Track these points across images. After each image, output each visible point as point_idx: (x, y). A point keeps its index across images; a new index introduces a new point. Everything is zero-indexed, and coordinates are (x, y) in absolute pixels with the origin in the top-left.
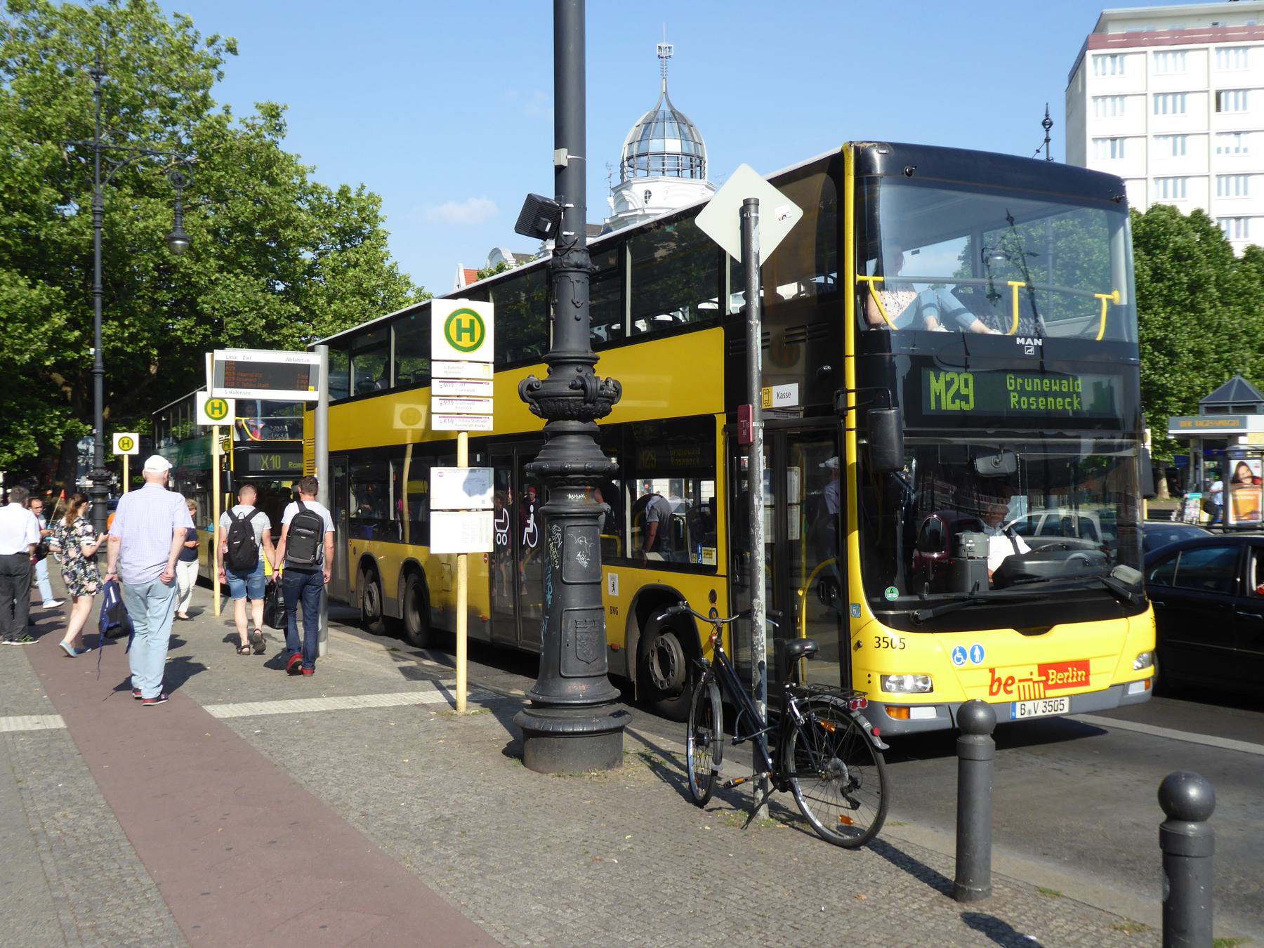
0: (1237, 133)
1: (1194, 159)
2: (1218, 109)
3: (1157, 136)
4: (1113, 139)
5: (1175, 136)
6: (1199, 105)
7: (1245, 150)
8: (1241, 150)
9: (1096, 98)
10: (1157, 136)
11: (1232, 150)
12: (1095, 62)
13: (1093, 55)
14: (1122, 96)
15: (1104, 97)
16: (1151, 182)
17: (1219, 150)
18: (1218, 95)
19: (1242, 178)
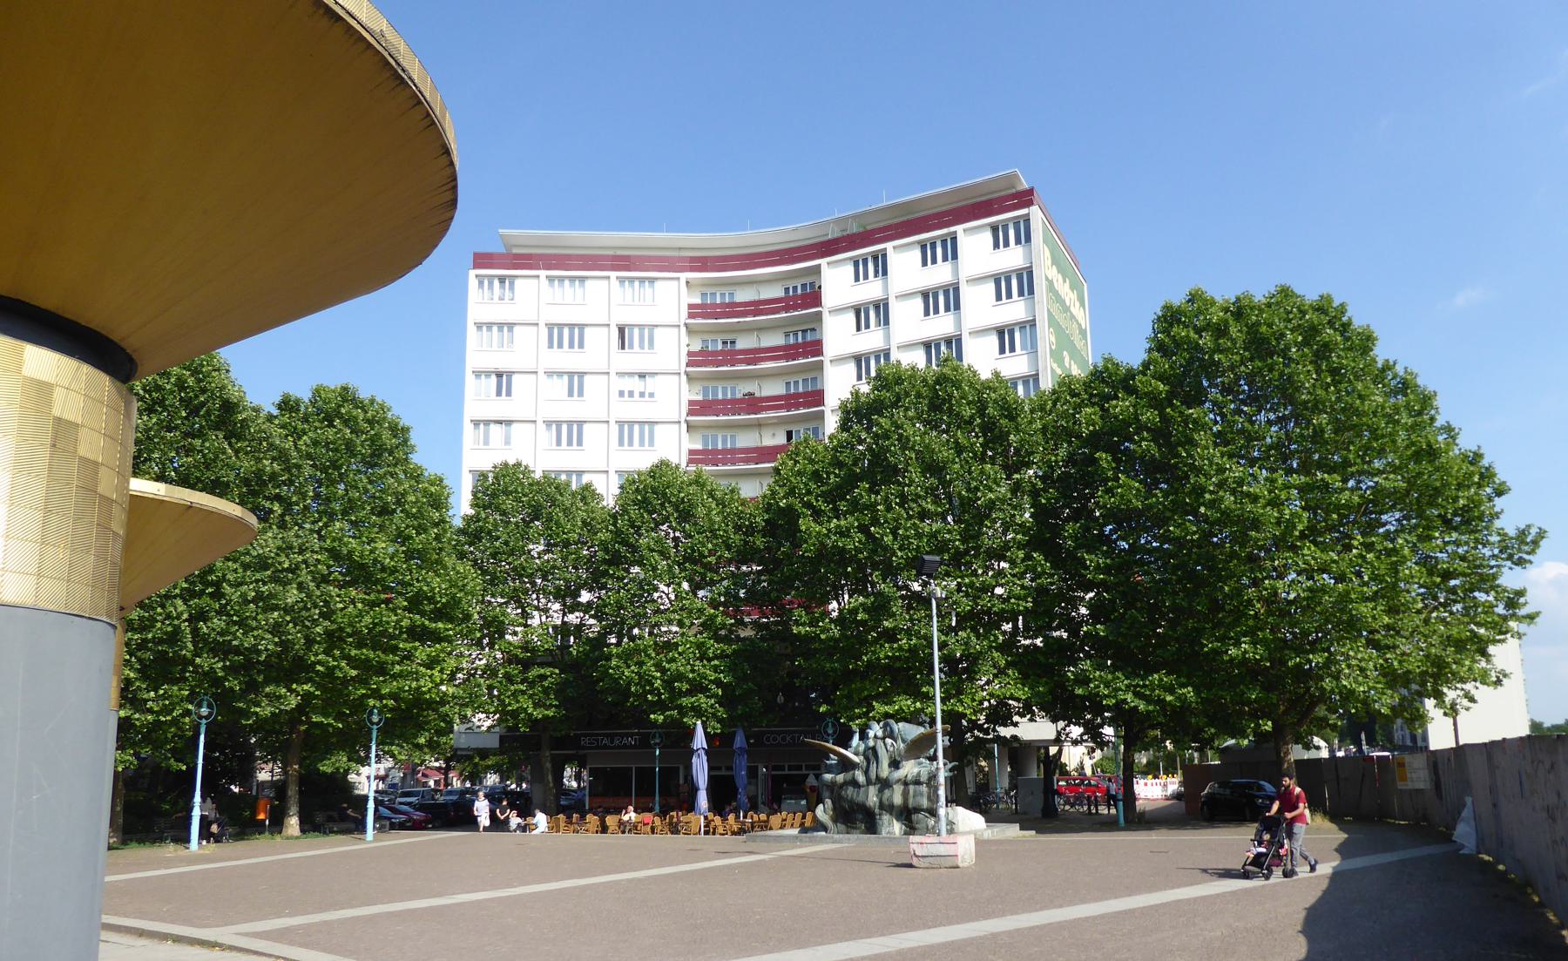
0: (642, 376)
1: (596, 401)
2: (623, 348)
3: (549, 374)
4: (499, 375)
5: (571, 374)
6: (600, 343)
7: (651, 395)
8: (647, 395)
9: (479, 326)
10: (549, 374)
11: (636, 395)
12: (481, 284)
13: (477, 276)
14: (511, 326)
15: (490, 325)
16: (541, 427)
17: (621, 394)
18: (621, 330)
19: (647, 427)
